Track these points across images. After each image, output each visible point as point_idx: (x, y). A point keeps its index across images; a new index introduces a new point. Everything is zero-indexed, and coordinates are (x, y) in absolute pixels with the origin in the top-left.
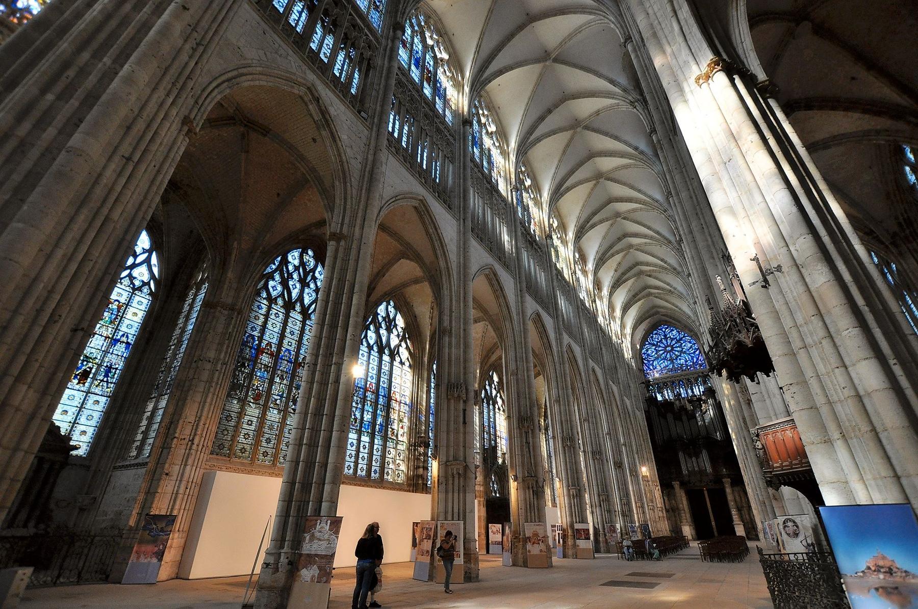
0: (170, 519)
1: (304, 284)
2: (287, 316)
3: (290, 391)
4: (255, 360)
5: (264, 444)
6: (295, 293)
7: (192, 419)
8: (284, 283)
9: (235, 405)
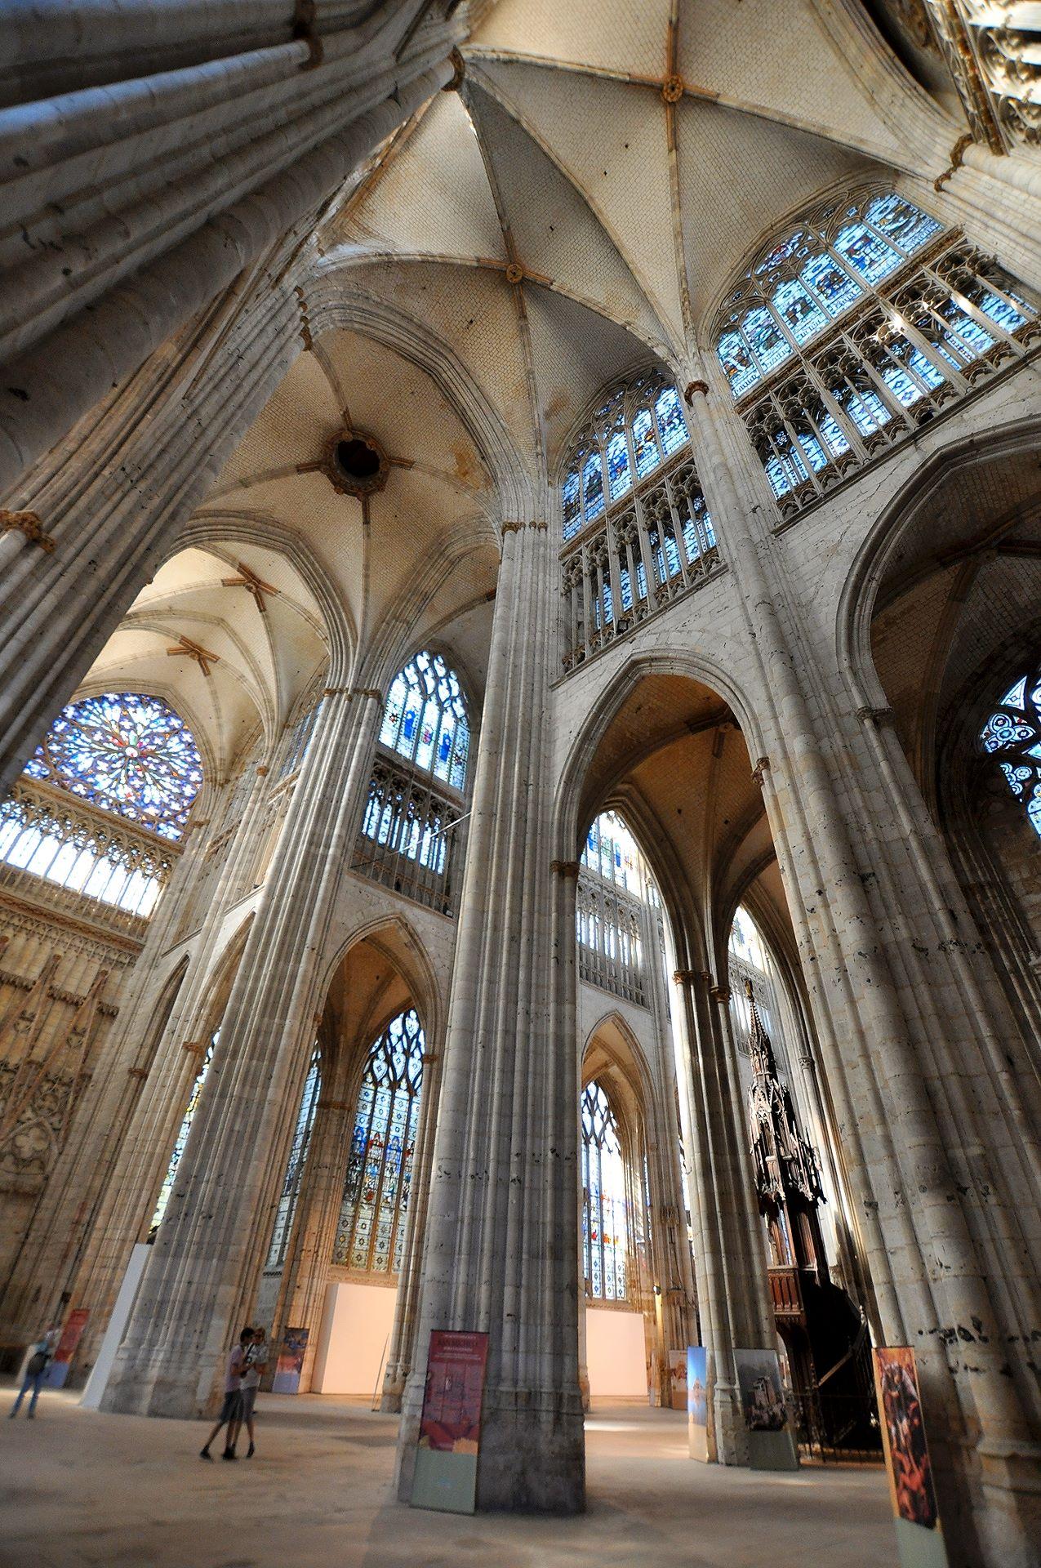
0: (304, 1332)
1: (408, 1053)
2: (393, 1097)
3: (400, 1185)
4: (364, 1155)
5: (378, 1249)
6: (399, 1070)
7: (315, 1229)
8: (389, 1061)
9: (349, 1209)
